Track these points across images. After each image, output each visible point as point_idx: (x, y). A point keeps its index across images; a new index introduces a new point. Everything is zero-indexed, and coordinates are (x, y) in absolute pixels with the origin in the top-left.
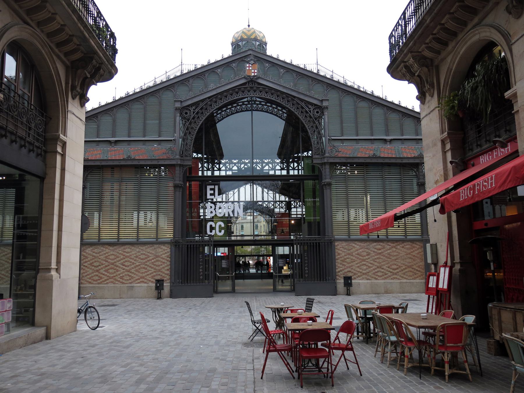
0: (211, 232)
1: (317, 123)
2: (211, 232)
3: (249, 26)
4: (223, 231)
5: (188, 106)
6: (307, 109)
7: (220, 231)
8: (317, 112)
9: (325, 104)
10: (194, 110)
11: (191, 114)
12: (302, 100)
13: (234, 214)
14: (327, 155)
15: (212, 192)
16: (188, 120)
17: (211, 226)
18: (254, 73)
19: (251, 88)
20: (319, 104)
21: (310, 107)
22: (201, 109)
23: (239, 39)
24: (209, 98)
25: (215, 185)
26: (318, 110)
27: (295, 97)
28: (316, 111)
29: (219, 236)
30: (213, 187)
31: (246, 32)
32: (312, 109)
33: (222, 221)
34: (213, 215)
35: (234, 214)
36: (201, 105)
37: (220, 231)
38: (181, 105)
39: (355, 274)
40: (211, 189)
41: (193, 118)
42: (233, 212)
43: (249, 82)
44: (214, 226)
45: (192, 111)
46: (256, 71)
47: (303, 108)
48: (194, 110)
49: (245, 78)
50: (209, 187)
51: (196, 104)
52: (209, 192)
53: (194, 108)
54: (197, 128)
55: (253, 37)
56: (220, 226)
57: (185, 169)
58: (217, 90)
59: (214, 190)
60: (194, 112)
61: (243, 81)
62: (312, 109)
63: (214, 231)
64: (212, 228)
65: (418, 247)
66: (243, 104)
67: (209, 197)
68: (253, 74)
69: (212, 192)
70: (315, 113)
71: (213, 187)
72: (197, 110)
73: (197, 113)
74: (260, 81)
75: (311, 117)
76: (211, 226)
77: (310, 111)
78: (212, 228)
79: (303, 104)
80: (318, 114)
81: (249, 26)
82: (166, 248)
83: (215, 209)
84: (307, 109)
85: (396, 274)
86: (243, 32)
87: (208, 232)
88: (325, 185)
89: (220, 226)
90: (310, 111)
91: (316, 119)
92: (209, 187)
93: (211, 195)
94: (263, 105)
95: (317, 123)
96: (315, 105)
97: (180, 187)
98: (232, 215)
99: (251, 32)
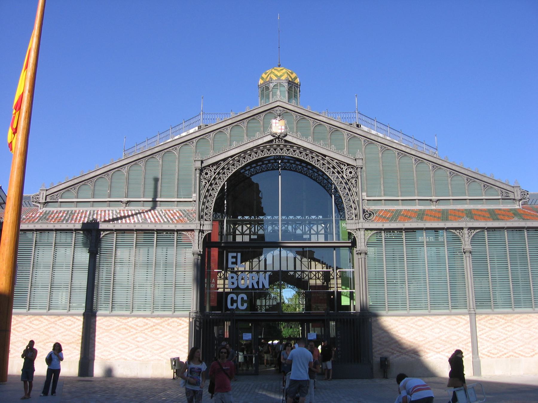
0: (232, 305)
2: (232, 305)
4: (246, 305)
5: (209, 166)
6: (339, 169)
7: (242, 305)
8: (351, 173)
10: (215, 170)
11: (211, 174)
12: (333, 159)
13: (258, 286)
15: (234, 260)
16: (209, 182)
17: (232, 298)
18: (281, 129)
19: (279, 145)
21: (342, 166)
22: (223, 168)
24: (231, 157)
25: (237, 252)
26: (351, 170)
27: (325, 156)
28: (348, 171)
29: (242, 310)
30: (235, 254)
33: (245, 293)
34: (235, 286)
35: (258, 286)
36: (223, 164)
37: (242, 305)
39: (393, 353)
40: (233, 257)
41: (215, 179)
42: (258, 283)
43: (275, 139)
44: (235, 298)
47: (334, 168)
48: (215, 170)
50: (230, 255)
51: (217, 163)
52: (231, 260)
53: (215, 167)
56: (242, 298)
57: (205, 234)
59: (236, 257)
60: (215, 173)
61: (270, 138)
62: (344, 170)
63: (235, 305)
64: (233, 301)
65: (464, 322)
66: (269, 163)
67: (230, 265)
69: (234, 260)
70: (348, 174)
71: (235, 254)
72: (218, 170)
73: (219, 173)
74: (288, 138)
75: (342, 177)
76: (232, 298)
77: (343, 172)
78: (233, 301)
80: (351, 175)
82: (183, 323)
83: (237, 280)
84: (339, 169)
85: (439, 352)
87: (229, 306)
89: (242, 298)
91: (349, 180)
92: (230, 255)
93: (233, 263)
94: (291, 163)
96: (348, 165)
98: (256, 287)
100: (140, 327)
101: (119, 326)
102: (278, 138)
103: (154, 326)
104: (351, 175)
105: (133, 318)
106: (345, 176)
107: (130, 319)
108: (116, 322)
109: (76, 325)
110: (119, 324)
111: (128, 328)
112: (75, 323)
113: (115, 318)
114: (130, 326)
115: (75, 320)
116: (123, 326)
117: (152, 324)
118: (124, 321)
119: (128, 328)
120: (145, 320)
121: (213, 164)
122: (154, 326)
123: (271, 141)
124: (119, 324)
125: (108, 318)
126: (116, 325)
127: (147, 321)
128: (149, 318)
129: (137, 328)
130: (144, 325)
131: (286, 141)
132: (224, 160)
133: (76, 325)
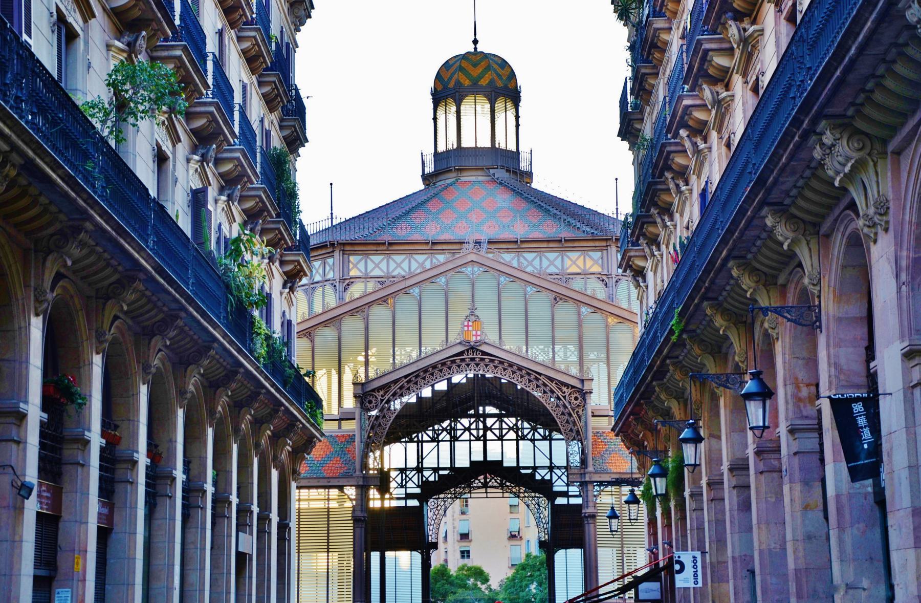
1: (575, 416)
3: (475, 42)
5: (373, 390)
8: (576, 399)
9: (586, 387)
12: (551, 379)
14: (590, 469)
18: (476, 335)
19: (473, 359)
20: (579, 386)
21: (564, 389)
23: (451, 85)
24: (406, 377)
27: (540, 374)
28: (573, 396)
31: (470, 69)
32: (567, 394)
36: (394, 388)
38: (363, 389)
43: (467, 350)
45: (379, 398)
46: (479, 333)
49: (460, 343)
53: (382, 393)
54: (388, 426)
55: (484, 82)
58: (418, 363)
68: (474, 339)
70: (573, 400)
72: (387, 397)
75: (565, 407)
79: (553, 386)
80: (577, 402)
81: (475, 42)
84: (560, 394)
86: (461, 69)
88: (587, 517)
90: (564, 397)
91: (573, 410)
95: (575, 416)
96: (573, 387)
97: (363, 521)
99: (479, 70)
102: (472, 348)
104: (577, 402)
106: (567, 405)
121: (379, 389)
123: (461, 353)
131: (484, 353)
132: (395, 382)
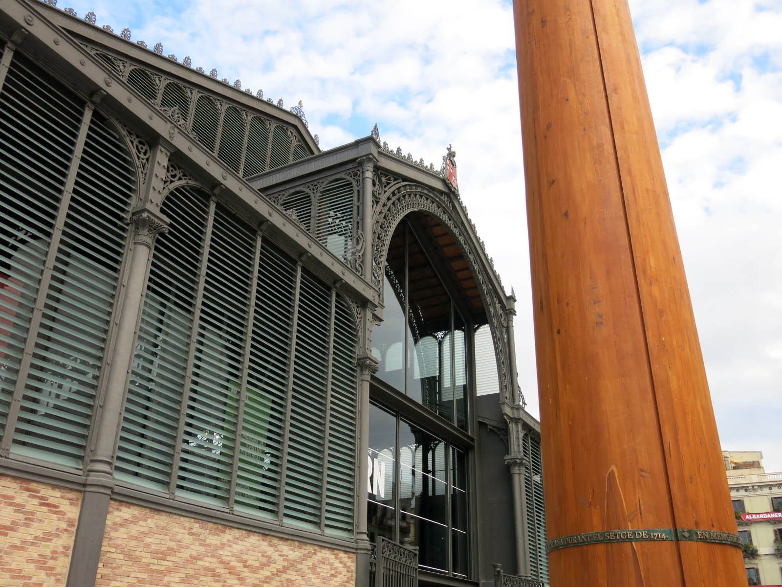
100: (254, 570)
101: (195, 558)
103: (285, 570)
105: (236, 533)
107: (230, 535)
108: (187, 539)
109: (36, 530)
110: (196, 549)
111: (220, 570)
112: (29, 519)
113: (187, 522)
114: (226, 564)
115: (32, 504)
116: (209, 562)
117: (280, 563)
118: (213, 540)
119: (220, 570)
120: (264, 545)
122: (285, 570)
124: (196, 549)
125: (162, 520)
126: (185, 554)
127: (270, 551)
128: (275, 541)
129: (246, 573)
130: (263, 566)
133: (36, 530)
